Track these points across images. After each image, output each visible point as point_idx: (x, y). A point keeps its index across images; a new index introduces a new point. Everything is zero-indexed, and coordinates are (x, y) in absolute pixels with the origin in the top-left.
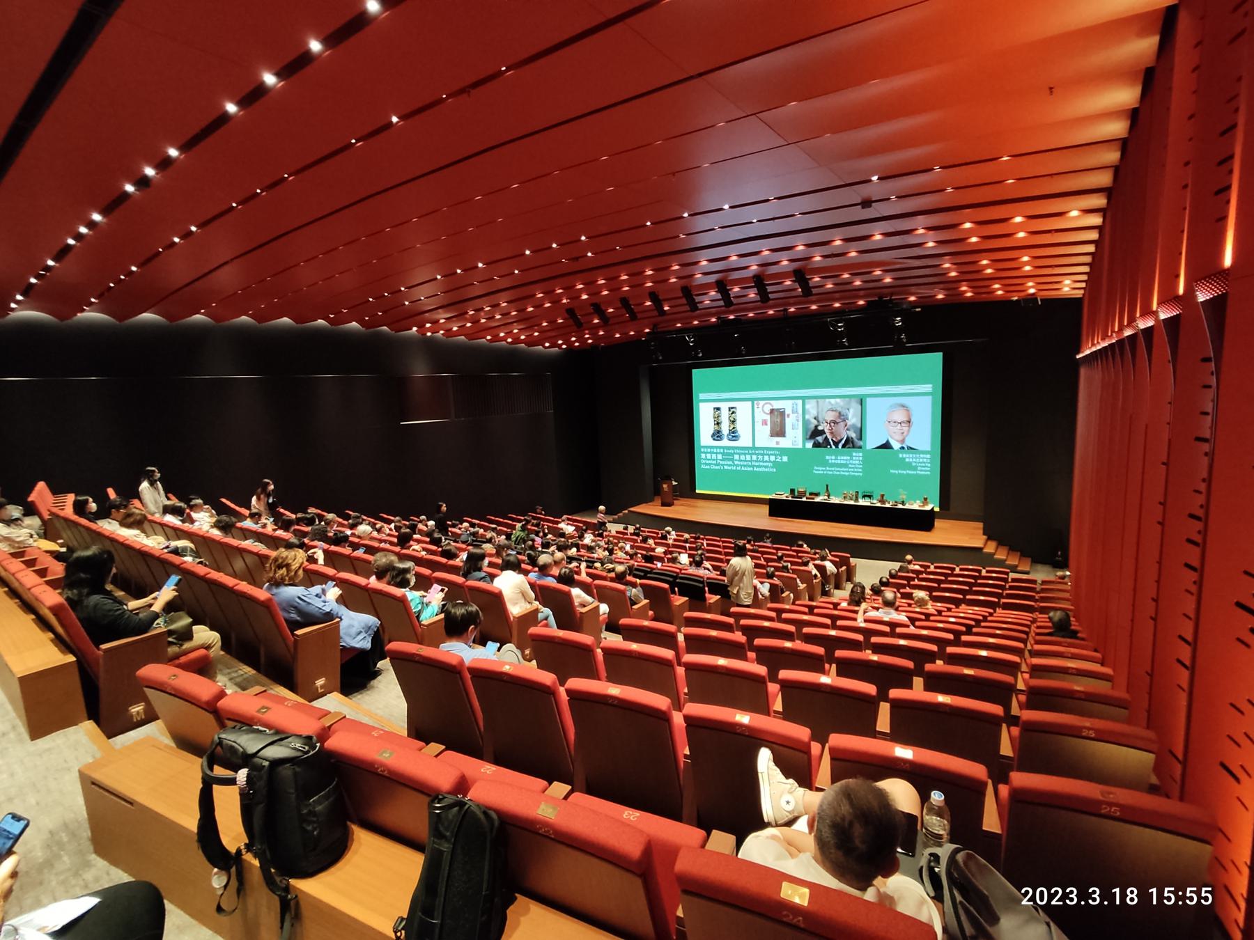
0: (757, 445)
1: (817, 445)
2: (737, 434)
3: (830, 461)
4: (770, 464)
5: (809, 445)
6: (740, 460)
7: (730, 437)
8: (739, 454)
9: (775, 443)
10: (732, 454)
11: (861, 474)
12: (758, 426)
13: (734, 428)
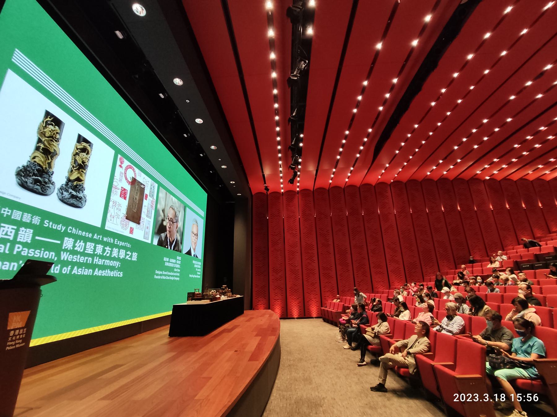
0: (109, 226)
1: (161, 243)
2: (80, 195)
3: (167, 264)
4: (117, 264)
5: (156, 242)
6: (73, 252)
7: (66, 194)
8: (76, 238)
9: (129, 230)
10: (61, 236)
11: (178, 279)
12: (116, 197)
13: (78, 179)
